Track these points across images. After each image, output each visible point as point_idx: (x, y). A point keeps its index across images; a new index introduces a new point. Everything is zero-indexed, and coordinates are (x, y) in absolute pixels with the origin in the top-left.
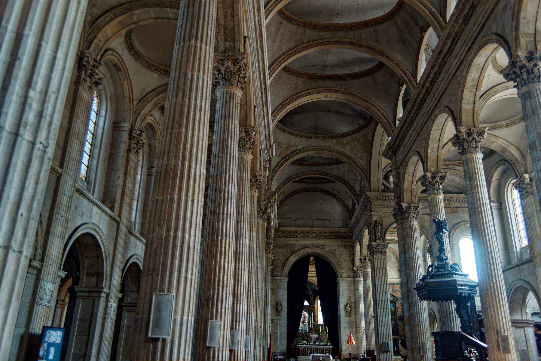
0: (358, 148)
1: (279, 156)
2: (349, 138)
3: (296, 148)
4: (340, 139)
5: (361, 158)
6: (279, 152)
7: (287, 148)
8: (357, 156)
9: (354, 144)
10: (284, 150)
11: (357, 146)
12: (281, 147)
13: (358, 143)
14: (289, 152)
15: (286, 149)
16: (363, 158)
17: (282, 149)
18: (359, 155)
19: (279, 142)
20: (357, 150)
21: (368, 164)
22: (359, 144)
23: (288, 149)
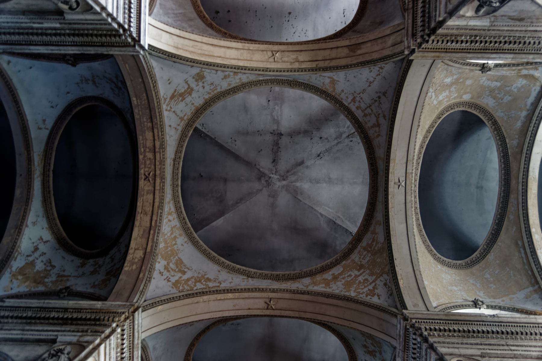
0: (361, 279)
2: (336, 270)
4: (317, 276)
5: (372, 293)
6: (176, 278)
8: (362, 294)
9: (350, 276)
10: (188, 280)
11: (356, 276)
12: (184, 273)
13: (359, 270)
14: (199, 286)
15: (193, 280)
16: (376, 291)
17: (185, 277)
18: (366, 289)
19: (182, 262)
20: (360, 282)
21: (391, 295)
22: (362, 270)
23: (200, 281)
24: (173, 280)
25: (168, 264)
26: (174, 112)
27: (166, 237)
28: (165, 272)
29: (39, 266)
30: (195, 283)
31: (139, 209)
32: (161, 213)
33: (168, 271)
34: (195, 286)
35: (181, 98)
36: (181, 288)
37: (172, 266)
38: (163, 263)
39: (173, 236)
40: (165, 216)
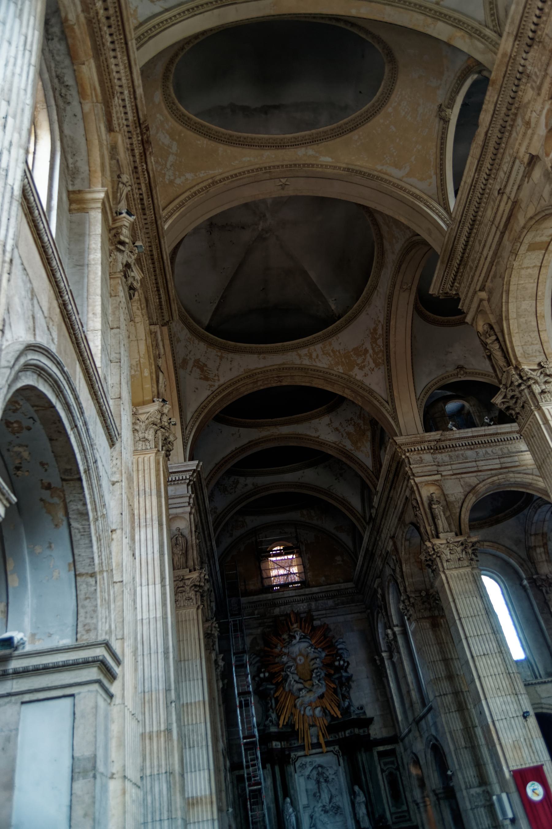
1: (377, 365)
3: (380, 327)
6: (371, 361)
7: (374, 341)
10: (373, 349)
12: (366, 351)
14: (380, 342)
15: (374, 345)
17: (371, 351)
19: (355, 350)
24: (372, 365)
25: (358, 365)
26: (218, 370)
27: (332, 362)
28: (366, 369)
29: (351, 429)
30: (377, 344)
31: (308, 384)
32: (311, 370)
33: (364, 366)
34: (380, 347)
35: (205, 368)
36: (380, 361)
37: (359, 361)
38: (356, 370)
39: (332, 354)
40: (314, 364)
